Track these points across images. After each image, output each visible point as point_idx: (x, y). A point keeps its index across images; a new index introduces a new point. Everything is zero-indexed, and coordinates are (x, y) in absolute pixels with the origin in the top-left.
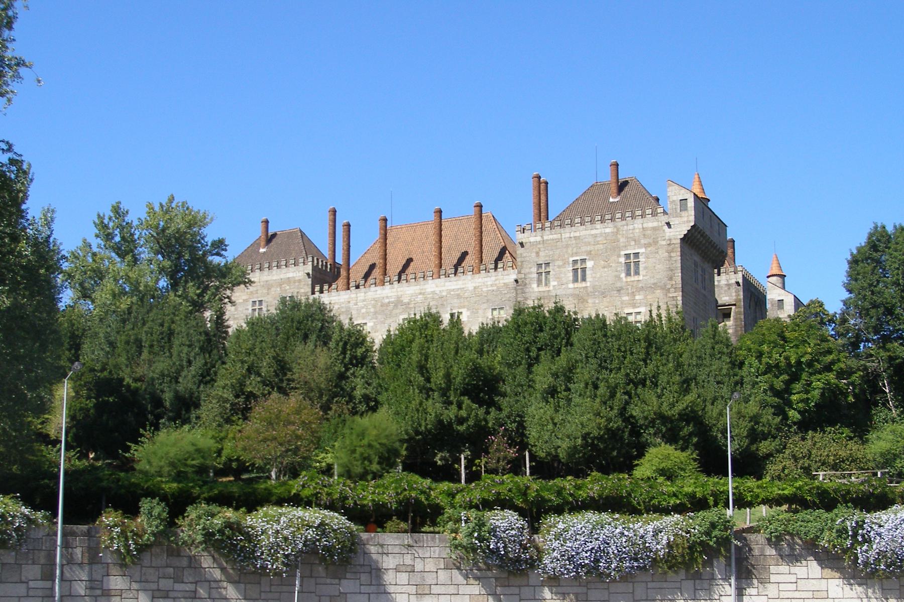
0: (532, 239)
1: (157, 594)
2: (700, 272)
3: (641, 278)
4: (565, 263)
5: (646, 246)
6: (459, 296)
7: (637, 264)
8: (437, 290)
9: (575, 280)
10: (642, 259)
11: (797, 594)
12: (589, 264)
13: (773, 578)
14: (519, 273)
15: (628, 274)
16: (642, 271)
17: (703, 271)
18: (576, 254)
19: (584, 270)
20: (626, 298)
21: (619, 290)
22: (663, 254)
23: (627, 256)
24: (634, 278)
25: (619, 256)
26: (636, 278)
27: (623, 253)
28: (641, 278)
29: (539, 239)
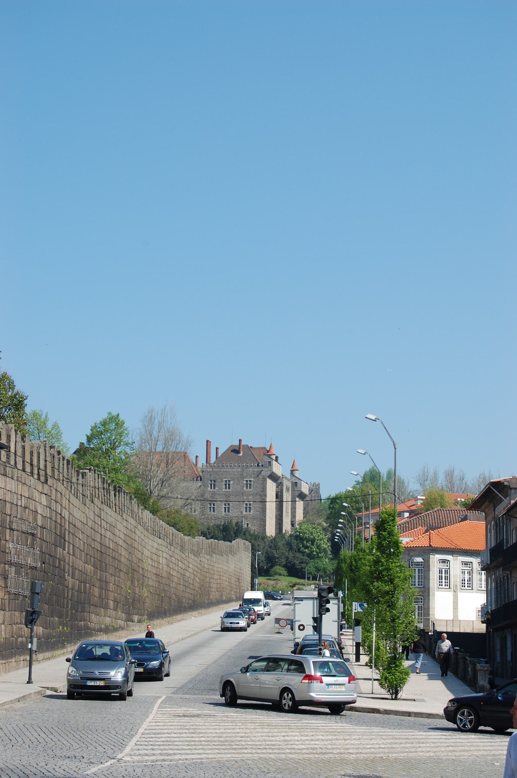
3: (251, 490)
9: (226, 488)
10: (252, 483)
12: (231, 482)
15: (247, 488)
16: (252, 488)
19: (229, 485)
25: (243, 480)
28: (251, 490)
29: (211, 470)
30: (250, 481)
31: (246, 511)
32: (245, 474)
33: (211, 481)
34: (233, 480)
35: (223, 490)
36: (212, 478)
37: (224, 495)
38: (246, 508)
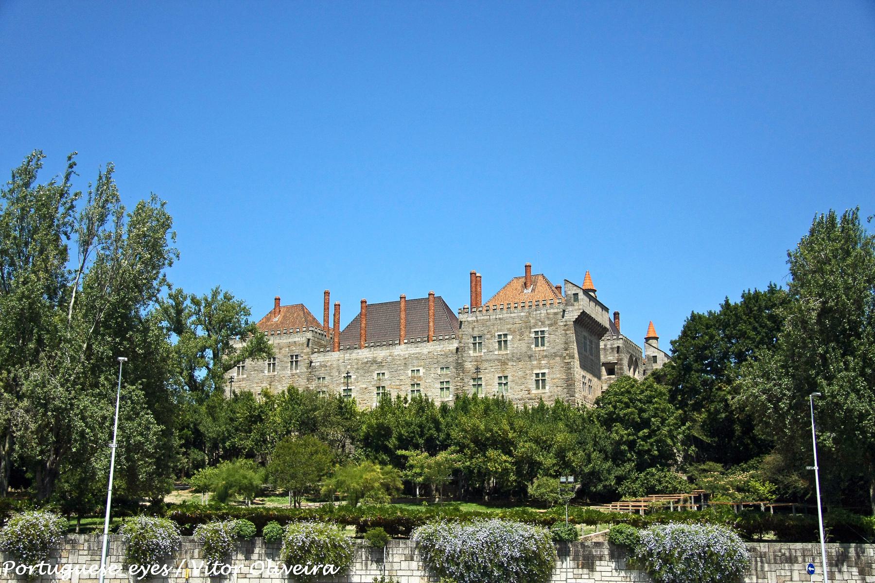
0: (470, 319)
1: (240, 576)
2: (588, 343)
3: (545, 348)
4: (493, 336)
5: (550, 325)
6: (417, 358)
7: (543, 338)
8: (402, 353)
9: (500, 349)
10: (546, 335)
11: (612, 579)
12: (509, 338)
13: (598, 569)
14: (460, 342)
15: (537, 346)
16: (546, 344)
17: (591, 342)
18: (501, 330)
19: (506, 342)
20: (535, 362)
21: (530, 357)
22: (561, 331)
23: (536, 332)
24: (540, 348)
25: (530, 332)
26: (541, 348)
27: (533, 330)
28: (545, 348)
29: (474, 319)
30: (542, 332)
31: (538, 388)
32: (533, 321)
33: (475, 338)
34: (513, 332)
35: (496, 353)
36: (476, 334)
37: (497, 360)
38: (537, 381)
